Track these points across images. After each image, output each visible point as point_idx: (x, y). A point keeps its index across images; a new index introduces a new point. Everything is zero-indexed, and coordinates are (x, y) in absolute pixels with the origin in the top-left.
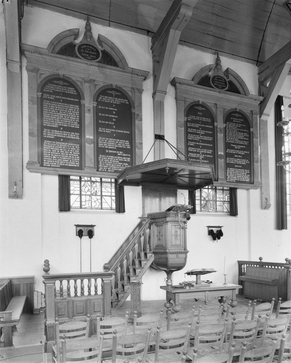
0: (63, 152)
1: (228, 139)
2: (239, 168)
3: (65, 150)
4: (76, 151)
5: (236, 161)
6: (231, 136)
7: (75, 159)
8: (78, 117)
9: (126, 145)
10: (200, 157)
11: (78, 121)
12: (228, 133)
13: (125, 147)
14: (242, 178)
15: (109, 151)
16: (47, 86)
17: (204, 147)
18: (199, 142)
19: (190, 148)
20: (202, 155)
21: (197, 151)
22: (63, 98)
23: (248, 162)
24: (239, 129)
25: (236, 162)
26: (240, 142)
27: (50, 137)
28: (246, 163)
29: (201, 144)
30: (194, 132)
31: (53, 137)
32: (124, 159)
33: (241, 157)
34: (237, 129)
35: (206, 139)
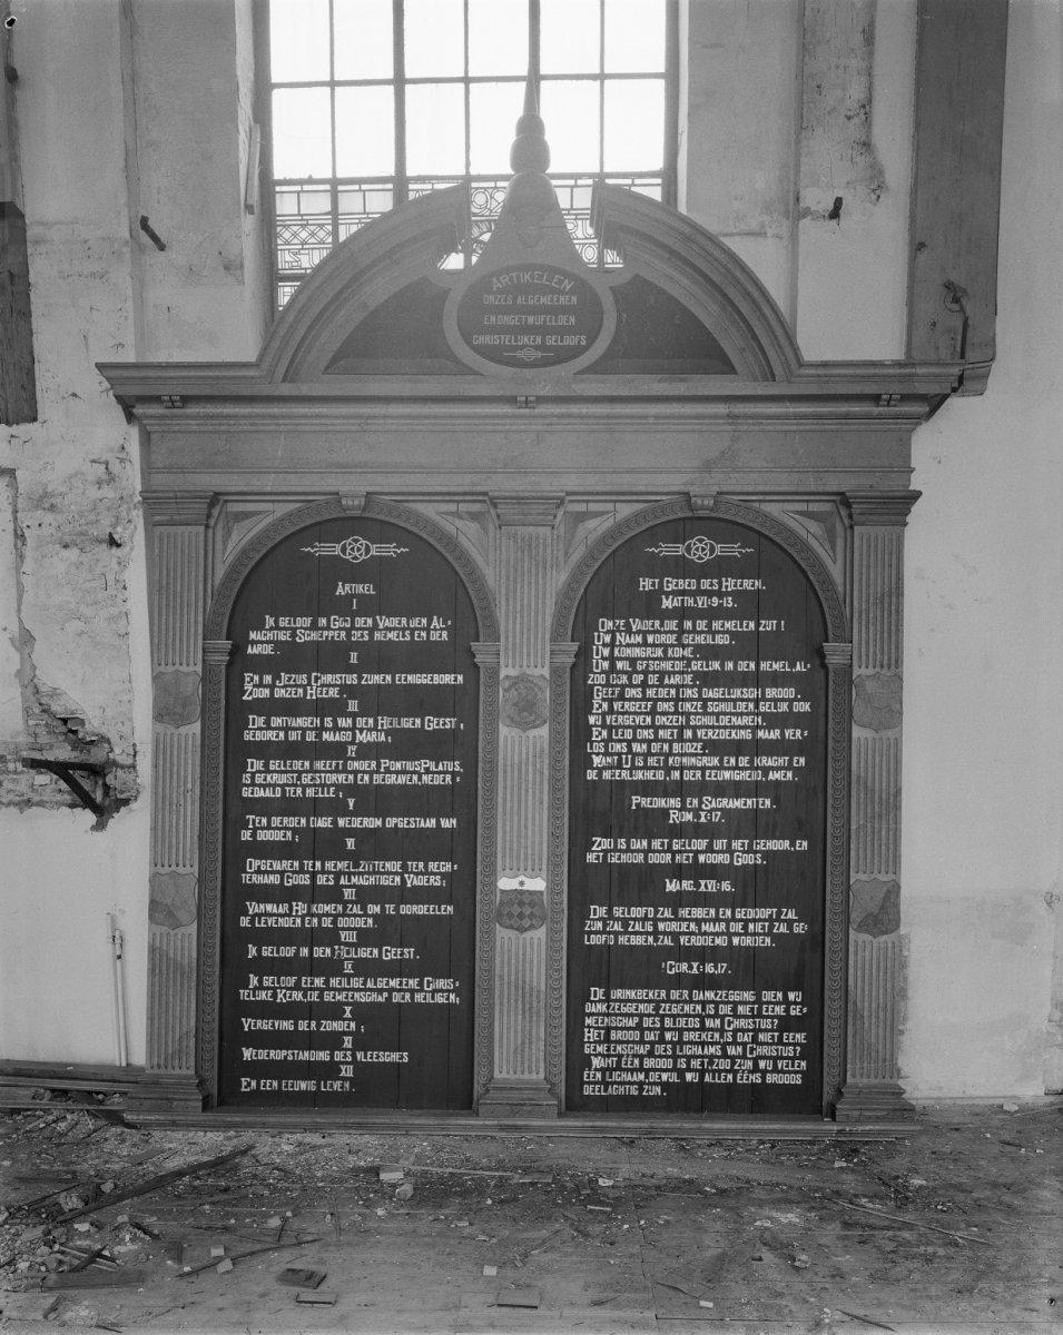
1: (606, 754)
2: (703, 982)
5: (674, 926)
6: (635, 728)
10: (342, 922)
12: (611, 711)
14: (724, 1064)
17: (376, 846)
18: (335, 808)
19: (255, 863)
20: (356, 909)
21: (321, 880)
23: (799, 928)
24: (716, 665)
25: (675, 936)
26: (721, 768)
28: (775, 938)
29: (356, 823)
30: (293, 736)
33: (726, 886)
34: (696, 666)
35: (402, 780)
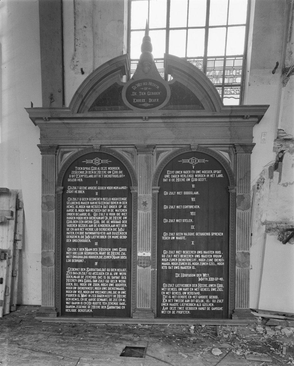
0: (99, 284)
3: (101, 281)
4: (120, 281)
7: (119, 296)
8: (126, 218)
9: (216, 260)
11: (126, 226)
13: (213, 264)
15: (180, 275)
16: (73, 172)
22: (99, 188)
27: (76, 261)
31: (81, 261)
32: (210, 288)
